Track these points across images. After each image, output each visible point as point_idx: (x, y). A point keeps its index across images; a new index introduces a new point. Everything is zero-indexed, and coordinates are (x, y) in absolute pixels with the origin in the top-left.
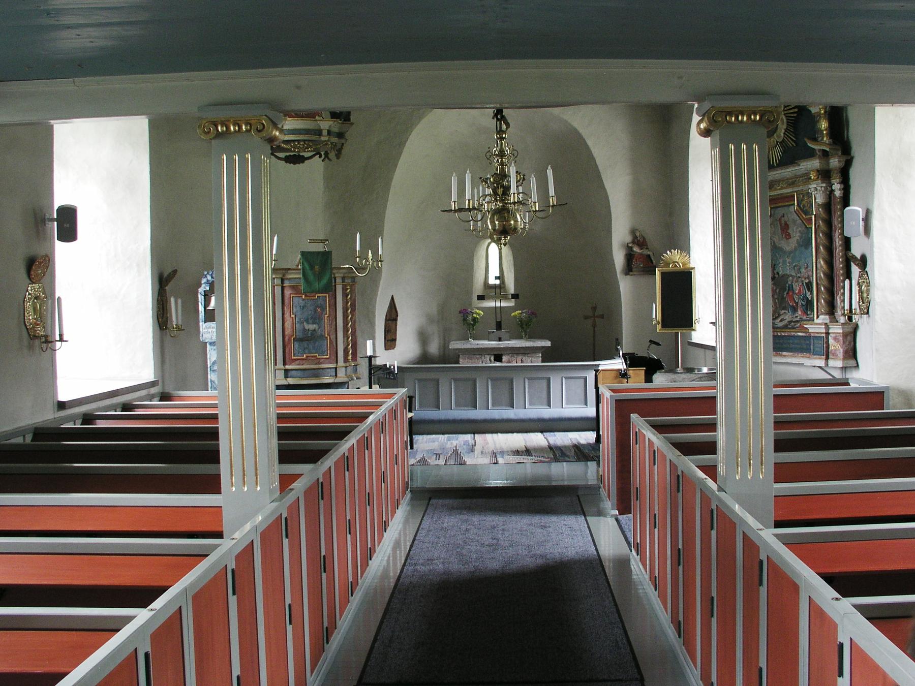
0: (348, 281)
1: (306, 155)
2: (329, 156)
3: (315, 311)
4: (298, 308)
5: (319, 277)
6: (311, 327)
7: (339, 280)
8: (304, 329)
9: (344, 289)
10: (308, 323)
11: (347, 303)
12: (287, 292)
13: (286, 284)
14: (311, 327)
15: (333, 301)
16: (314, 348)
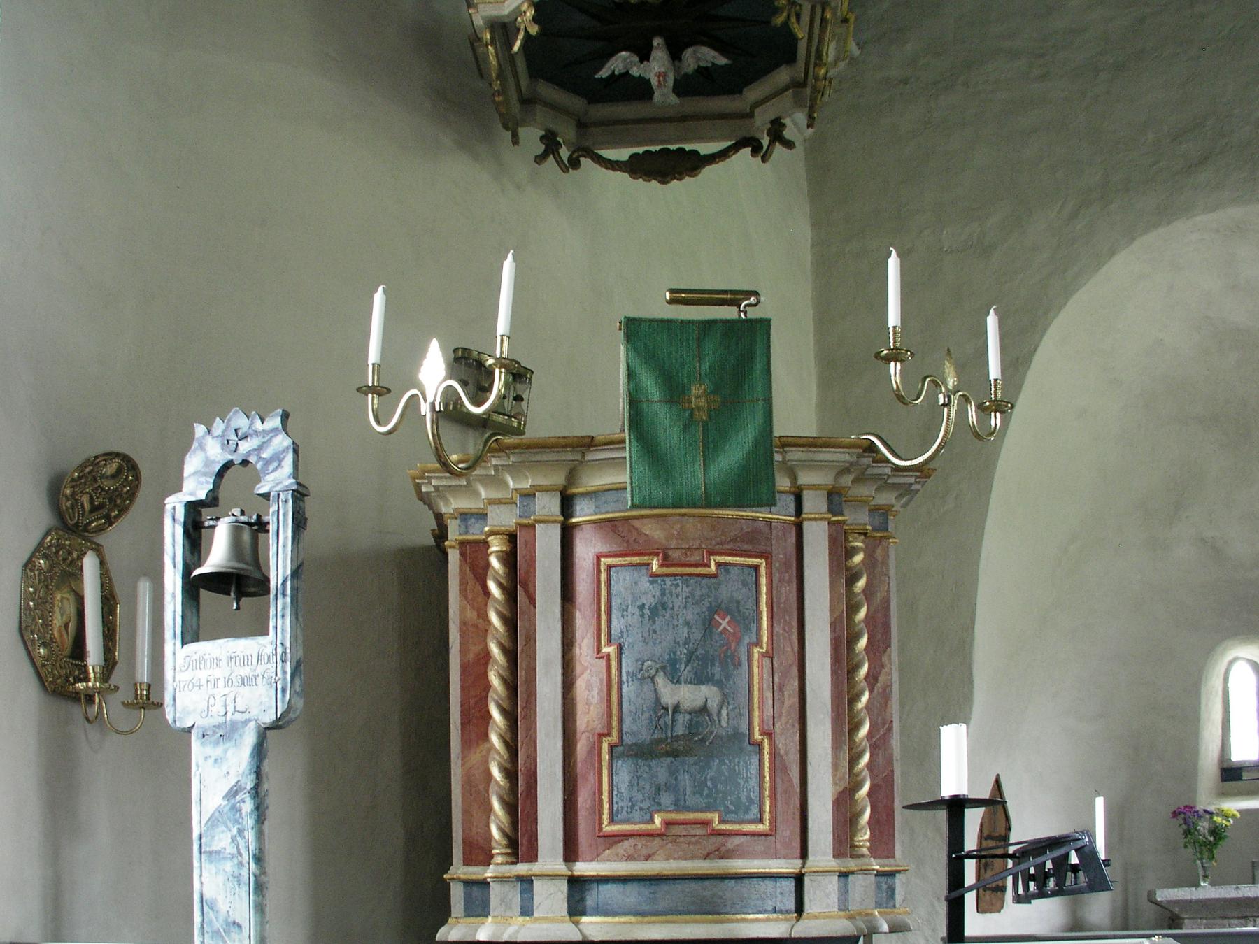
0: (856, 517)
1: (705, 148)
2: (787, 134)
3: (709, 625)
4: (633, 617)
5: (711, 434)
6: (689, 695)
7: (814, 503)
8: (658, 706)
9: (840, 551)
10: (675, 679)
11: (852, 609)
12: (586, 549)
13: (583, 513)
14: (689, 695)
15: (789, 591)
16: (700, 786)
